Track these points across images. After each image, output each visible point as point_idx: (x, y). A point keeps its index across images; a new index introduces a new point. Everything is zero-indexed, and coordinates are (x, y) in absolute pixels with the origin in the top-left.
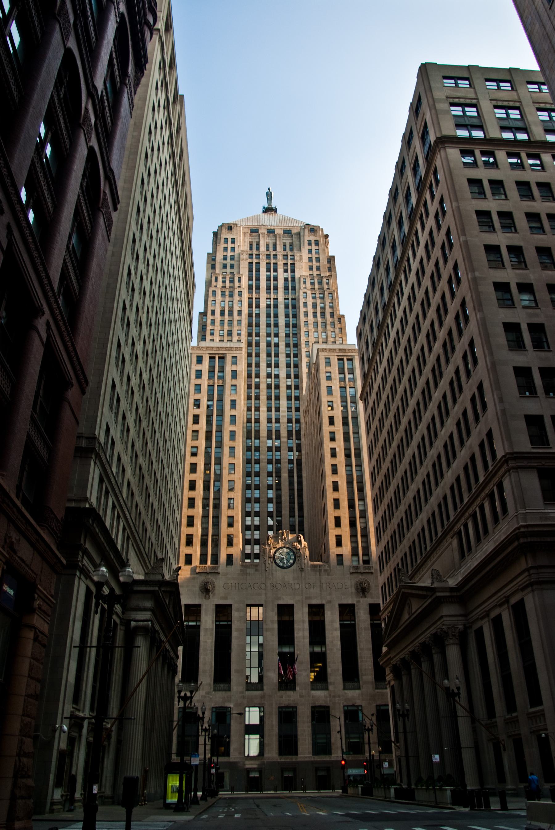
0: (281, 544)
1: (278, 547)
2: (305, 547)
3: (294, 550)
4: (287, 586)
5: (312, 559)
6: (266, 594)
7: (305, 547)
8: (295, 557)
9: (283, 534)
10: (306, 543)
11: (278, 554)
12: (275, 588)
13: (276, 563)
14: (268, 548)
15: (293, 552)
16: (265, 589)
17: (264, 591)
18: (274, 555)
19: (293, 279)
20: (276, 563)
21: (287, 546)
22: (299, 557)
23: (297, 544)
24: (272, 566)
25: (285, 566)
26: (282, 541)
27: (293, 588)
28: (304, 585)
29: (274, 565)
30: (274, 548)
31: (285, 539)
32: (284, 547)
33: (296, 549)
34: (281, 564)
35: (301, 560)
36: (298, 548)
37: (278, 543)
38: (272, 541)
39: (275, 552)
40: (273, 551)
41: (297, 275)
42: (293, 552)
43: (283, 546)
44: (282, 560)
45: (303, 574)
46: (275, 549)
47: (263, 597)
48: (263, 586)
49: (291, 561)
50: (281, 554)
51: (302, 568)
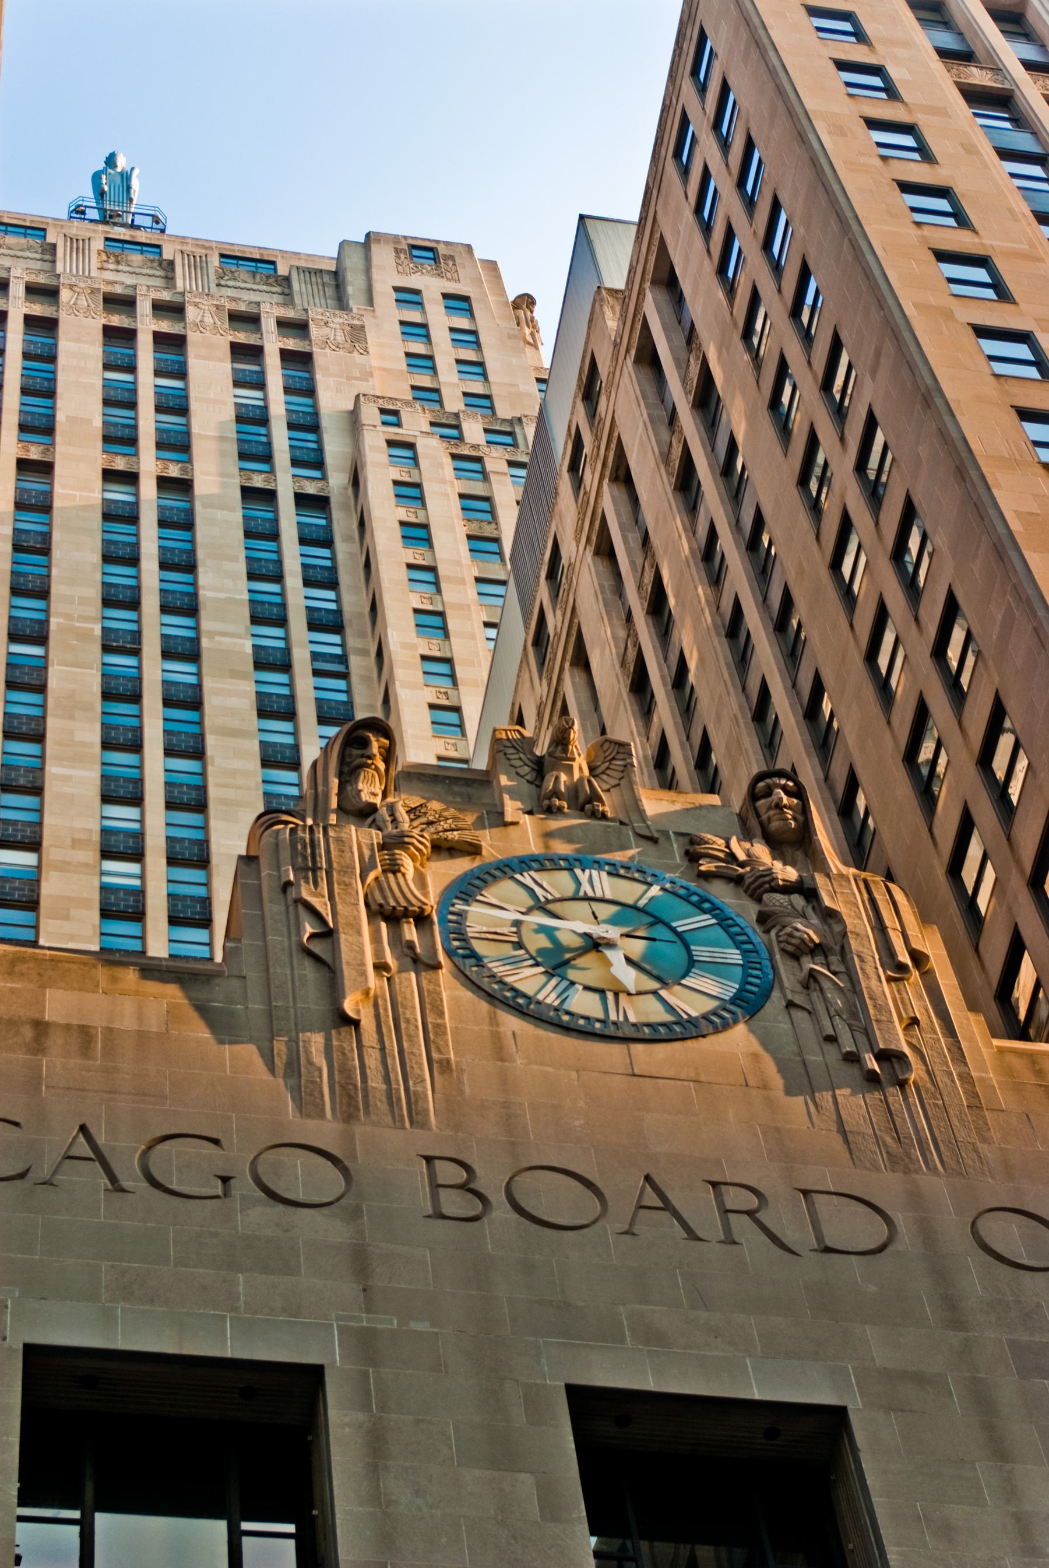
12: (501, 1212)
19: (306, 424)
24: (430, 1003)
30: (442, 849)
41: (332, 399)
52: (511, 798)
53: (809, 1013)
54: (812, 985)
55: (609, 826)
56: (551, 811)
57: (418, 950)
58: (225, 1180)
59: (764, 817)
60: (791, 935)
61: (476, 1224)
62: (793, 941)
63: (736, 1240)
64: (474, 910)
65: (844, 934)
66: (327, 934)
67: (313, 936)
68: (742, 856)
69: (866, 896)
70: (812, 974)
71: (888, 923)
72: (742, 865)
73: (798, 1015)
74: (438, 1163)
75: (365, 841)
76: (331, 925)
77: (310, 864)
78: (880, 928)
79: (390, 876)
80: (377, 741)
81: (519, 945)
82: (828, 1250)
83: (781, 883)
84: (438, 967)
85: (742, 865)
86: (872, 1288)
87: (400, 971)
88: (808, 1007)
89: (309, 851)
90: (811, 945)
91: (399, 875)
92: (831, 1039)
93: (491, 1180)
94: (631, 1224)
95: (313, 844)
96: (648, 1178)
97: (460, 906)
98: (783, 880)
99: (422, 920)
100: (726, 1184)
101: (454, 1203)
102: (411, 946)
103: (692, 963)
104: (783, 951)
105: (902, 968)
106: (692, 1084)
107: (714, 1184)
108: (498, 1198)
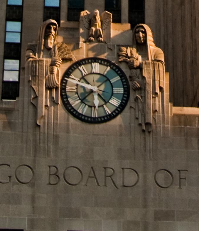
0: (84, 50)
1: (75, 59)
2: (156, 60)
3: (124, 67)
4: (100, 174)
5: (176, 101)
6: (33, 199)
7: (156, 60)
8: (127, 91)
9: (91, 21)
10: (160, 51)
11: (74, 80)
12: (62, 182)
13: (67, 105)
14: (46, 61)
15: (122, 75)
16: (31, 184)
17: (26, 190)
18: (64, 82)
20: (67, 105)
21: (103, 56)
22: (140, 89)
23: (132, 52)
24: (56, 114)
25: (95, 114)
26: (88, 41)
27: (119, 183)
28: (150, 177)
29: (61, 111)
30: (65, 60)
31: (97, 36)
32: (95, 60)
33: (131, 66)
34: (83, 110)
35: (144, 97)
36: (136, 64)
37: (77, 47)
38: (60, 39)
39: (67, 74)
40: (60, 69)
42: (122, 75)
43: (91, 55)
44: (85, 96)
45: (150, 139)
46: (68, 65)
47: (26, 207)
48: (25, 174)
49: (115, 102)
50: (83, 78)
51: (148, 124)
52: (82, 38)
53: (134, 109)
54: (137, 101)
55: (102, 45)
56: (90, 41)
57: (55, 99)
58: (10, 177)
59: (137, 39)
60: (134, 85)
61: (56, 185)
62: (135, 87)
63: (107, 185)
64: (69, 80)
65: (145, 84)
66: (36, 97)
67: (33, 98)
68: (129, 55)
69: (153, 69)
70: (137, 97)
71: (156, 79)
72: (129, 58)
73: (132, 110)
74: (51, 167)
75: (47, 65)
76: (37, 95)
77: (34, 74)
78: (154, 81)
79: (51, 75)
80: (53, 26)
81: (77, 93)
82: (124, 186)
83: (135, 67)
84: (58, 104)
85: (129, 58)
86: (131, 197)
87: (51, 106)
88: (135, 108)
89: (35, 70)
90: (138, 88)
91: (53, 74)
92: (137, 118)
93: (61, 171)
94: (86, 183)
95: (36, 66)
96: (92, 168)
97: (66, 79)
98: (136, 66)
99: (57, 88)
100: (108, 168)
101: (53, 180)
102: (53, 98)
103: (112, 94)
104: (133, 88)
105: (156, 94)
106: (106, 136)
107: (105, 168)
108: (62, 177)
